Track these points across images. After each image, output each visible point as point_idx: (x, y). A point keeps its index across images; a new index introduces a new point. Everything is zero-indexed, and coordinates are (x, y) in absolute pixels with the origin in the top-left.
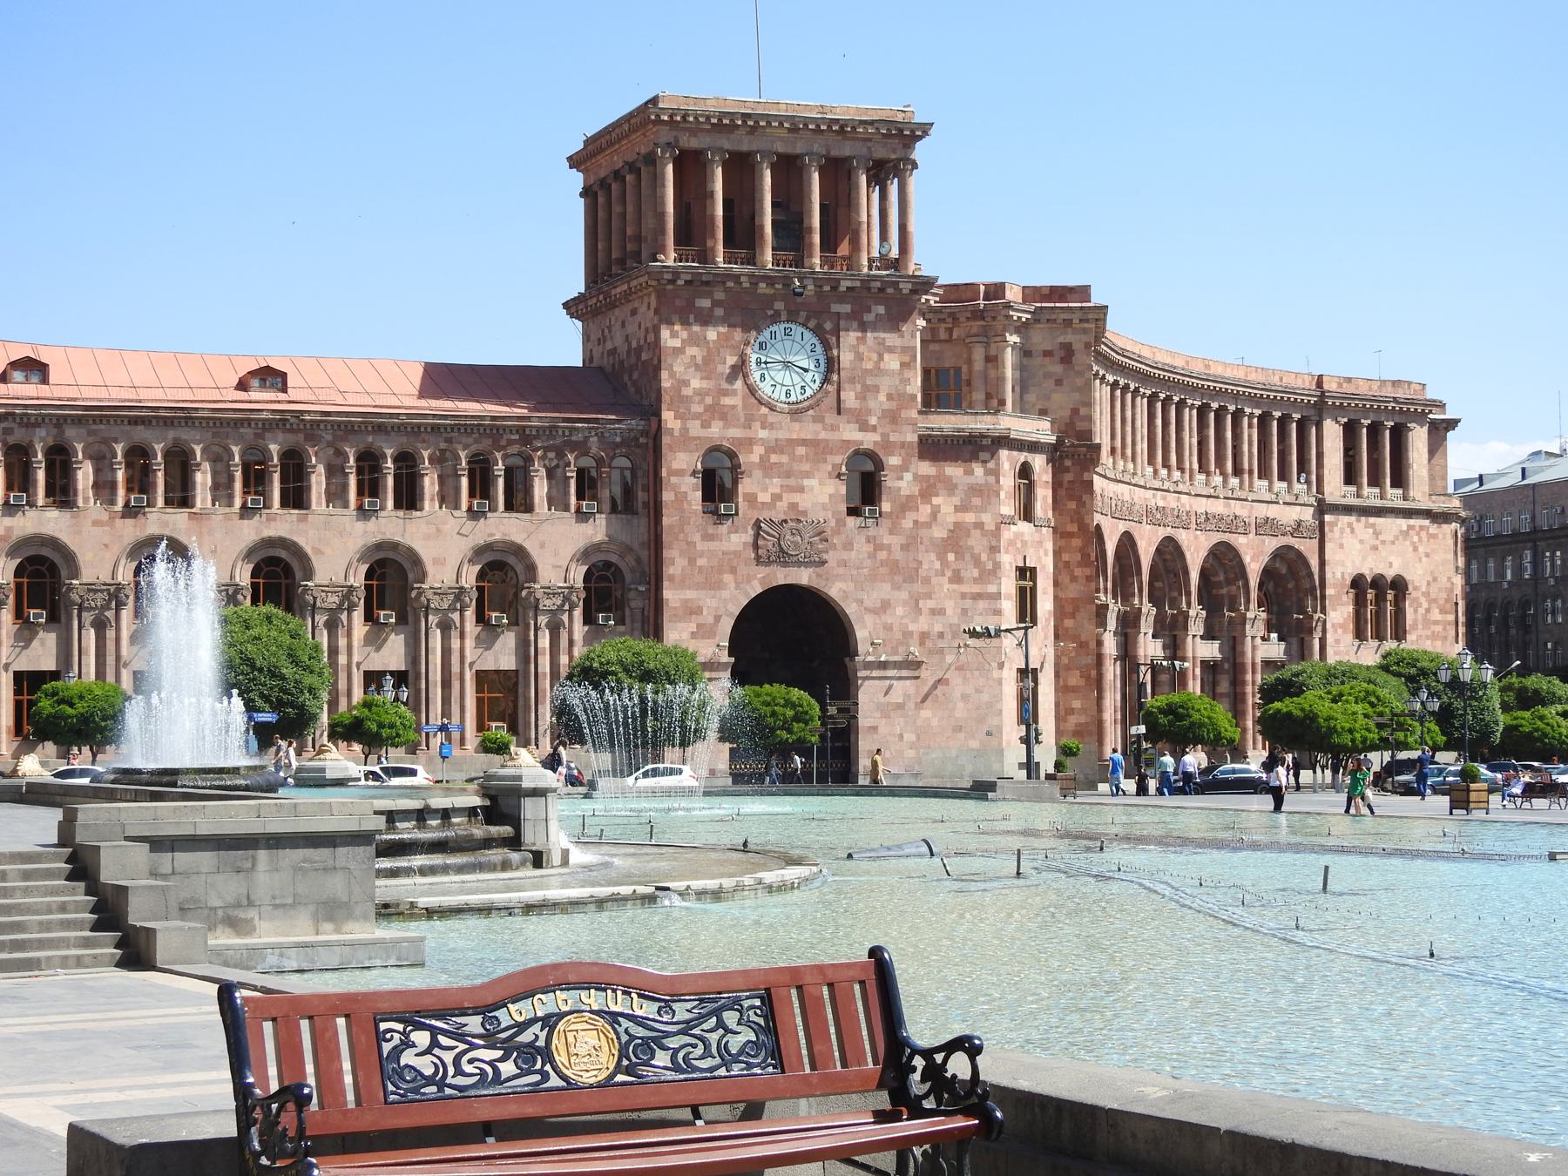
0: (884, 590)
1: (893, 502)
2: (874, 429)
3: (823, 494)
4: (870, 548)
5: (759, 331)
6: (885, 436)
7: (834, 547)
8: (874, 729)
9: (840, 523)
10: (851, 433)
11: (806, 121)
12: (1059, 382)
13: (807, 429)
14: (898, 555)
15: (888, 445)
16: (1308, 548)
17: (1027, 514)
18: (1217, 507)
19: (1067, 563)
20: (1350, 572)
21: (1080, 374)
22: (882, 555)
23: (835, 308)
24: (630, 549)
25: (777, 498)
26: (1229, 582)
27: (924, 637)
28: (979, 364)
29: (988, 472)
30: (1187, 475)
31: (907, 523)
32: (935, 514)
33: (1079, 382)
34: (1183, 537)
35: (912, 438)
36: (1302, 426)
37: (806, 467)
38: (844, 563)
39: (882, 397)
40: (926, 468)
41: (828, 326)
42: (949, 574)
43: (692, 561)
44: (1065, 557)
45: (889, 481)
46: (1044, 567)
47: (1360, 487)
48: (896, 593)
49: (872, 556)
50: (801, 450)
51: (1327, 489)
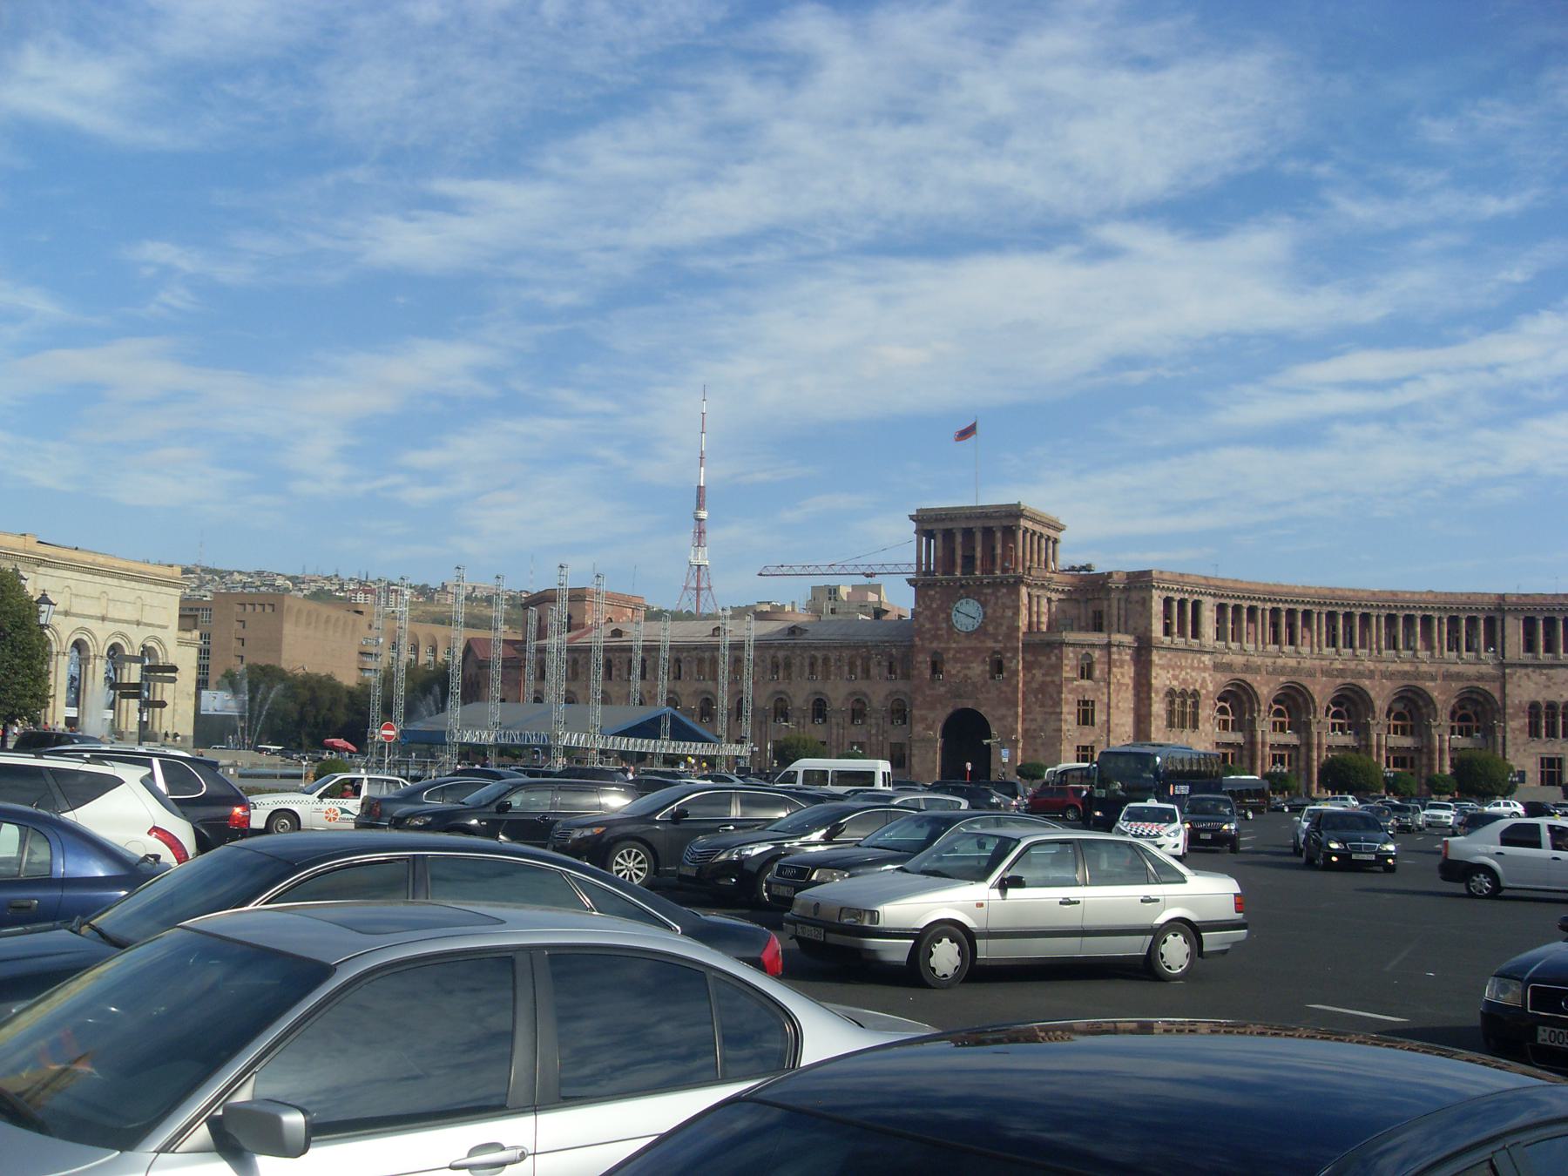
0: (1002, 711)
3: (978, 669)
10: (990, 644)
13: (974, 643)
16: (1492, 688)
17: (1090, 677)
18: (1407, 667)
26: (1426, 706)
30: (1375, 652)
34: (1366, 683)
36: (1490, 622)
40: (1029, 658)
47: (1537, 653)
51: (1507, 655)
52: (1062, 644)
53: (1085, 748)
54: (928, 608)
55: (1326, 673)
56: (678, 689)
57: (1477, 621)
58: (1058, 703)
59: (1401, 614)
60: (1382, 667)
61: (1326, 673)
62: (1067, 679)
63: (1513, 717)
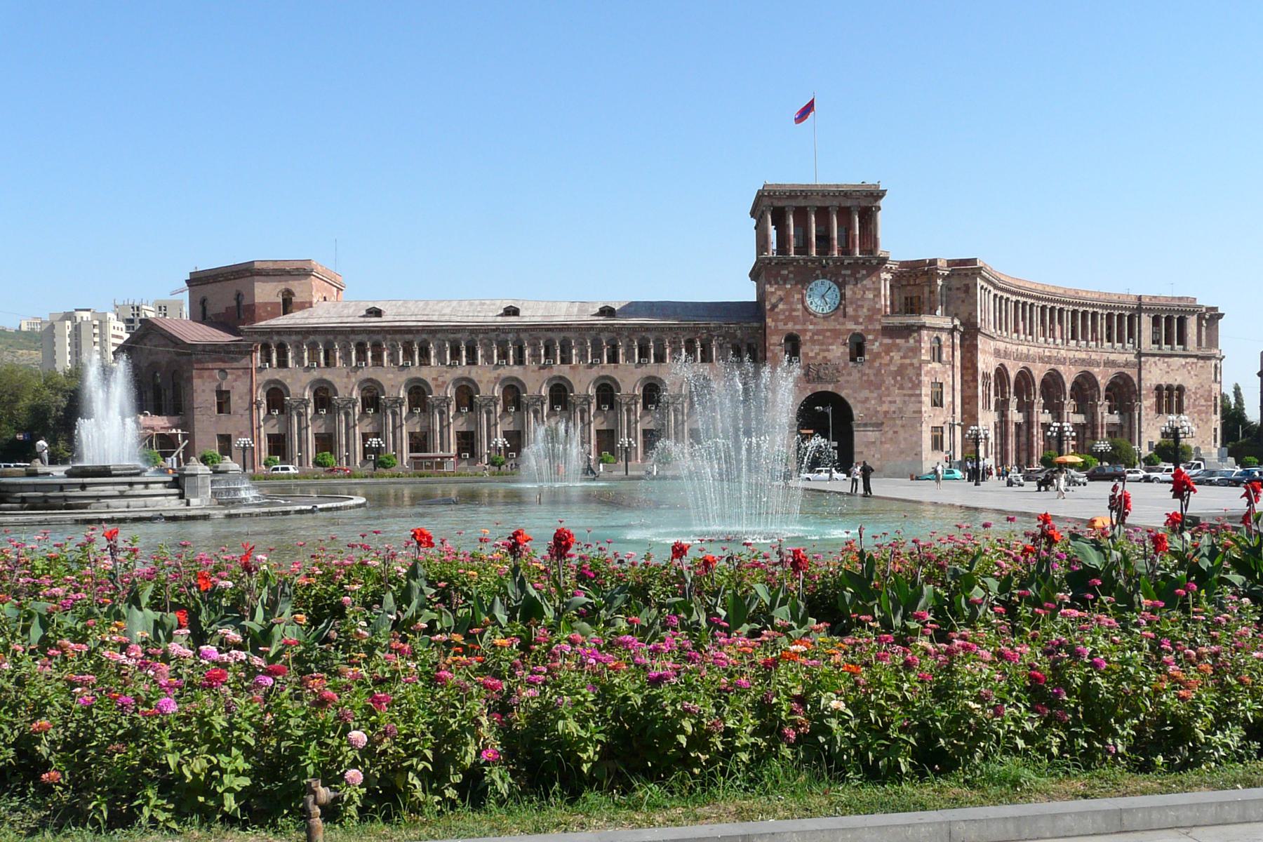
0: (866, 393)
3: (838, 352)
4: (858, 375)
9: (846, 365)
10: (851, 326)
11: (829, 192)
13: (832, 325)
14: (872, 378)
15: (869, 332)
18: (1083, 355)
20: (1154, 383)
22: (865, 378)
25: (817, 354)
26: (1091, 388)
27: (886, 413)
28: (926, 295)
31: (877, 364)
32: (891, 360)
35: (878, 327)
36: (1131, 318)
40: (887, 341)
45: (868, 346)
49: (861, 378)
50: (828, 334)
52: (923, 327)
53: (935, 428)
55: (1041, 359)
56: (473, 376)
57: (1120, 320)
58: (918, 385)
59: (1081, 309)
60: (1071, 355)
61: (1041, 359)
63: (1147, 396)
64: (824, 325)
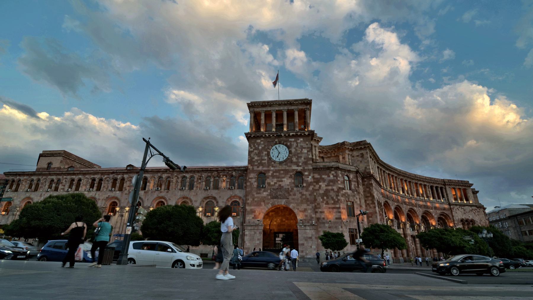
0: (304, 206)
1: (306, 183)
2: (301, 166)
3: (287, 182)
4: (300, 195)
5: (272, 146)
6: (304, 168)
7: (291, 195)
8: (303, 244)
10: (295, 167)
12: (361, 162)
13: (284, 167)
14: (308, 197)
15: (305, 170)
19: (368, 204)
21: (366, 159)
22: (304, 197)
23: (290, 140)
24: (240, 198)
25: (275, 183)
29: (334, 176)
31: (311, 188)
33: (366, 161)
34: (415, 208)
35: (311, 168)
36: (441, 188)
37: (283, 176)
38: (293, 199)
39: (303, 159)
40: (317, 176)
41: (289, 144)
42: (325, 202)
43: (253, 199)
44: (368, 202)
46: (356, 202)
48: (308, 207)
49: (301, 197)
50: (282, 172)
54: (256, 149)
62: (340, 188)
64: (280, 167)
